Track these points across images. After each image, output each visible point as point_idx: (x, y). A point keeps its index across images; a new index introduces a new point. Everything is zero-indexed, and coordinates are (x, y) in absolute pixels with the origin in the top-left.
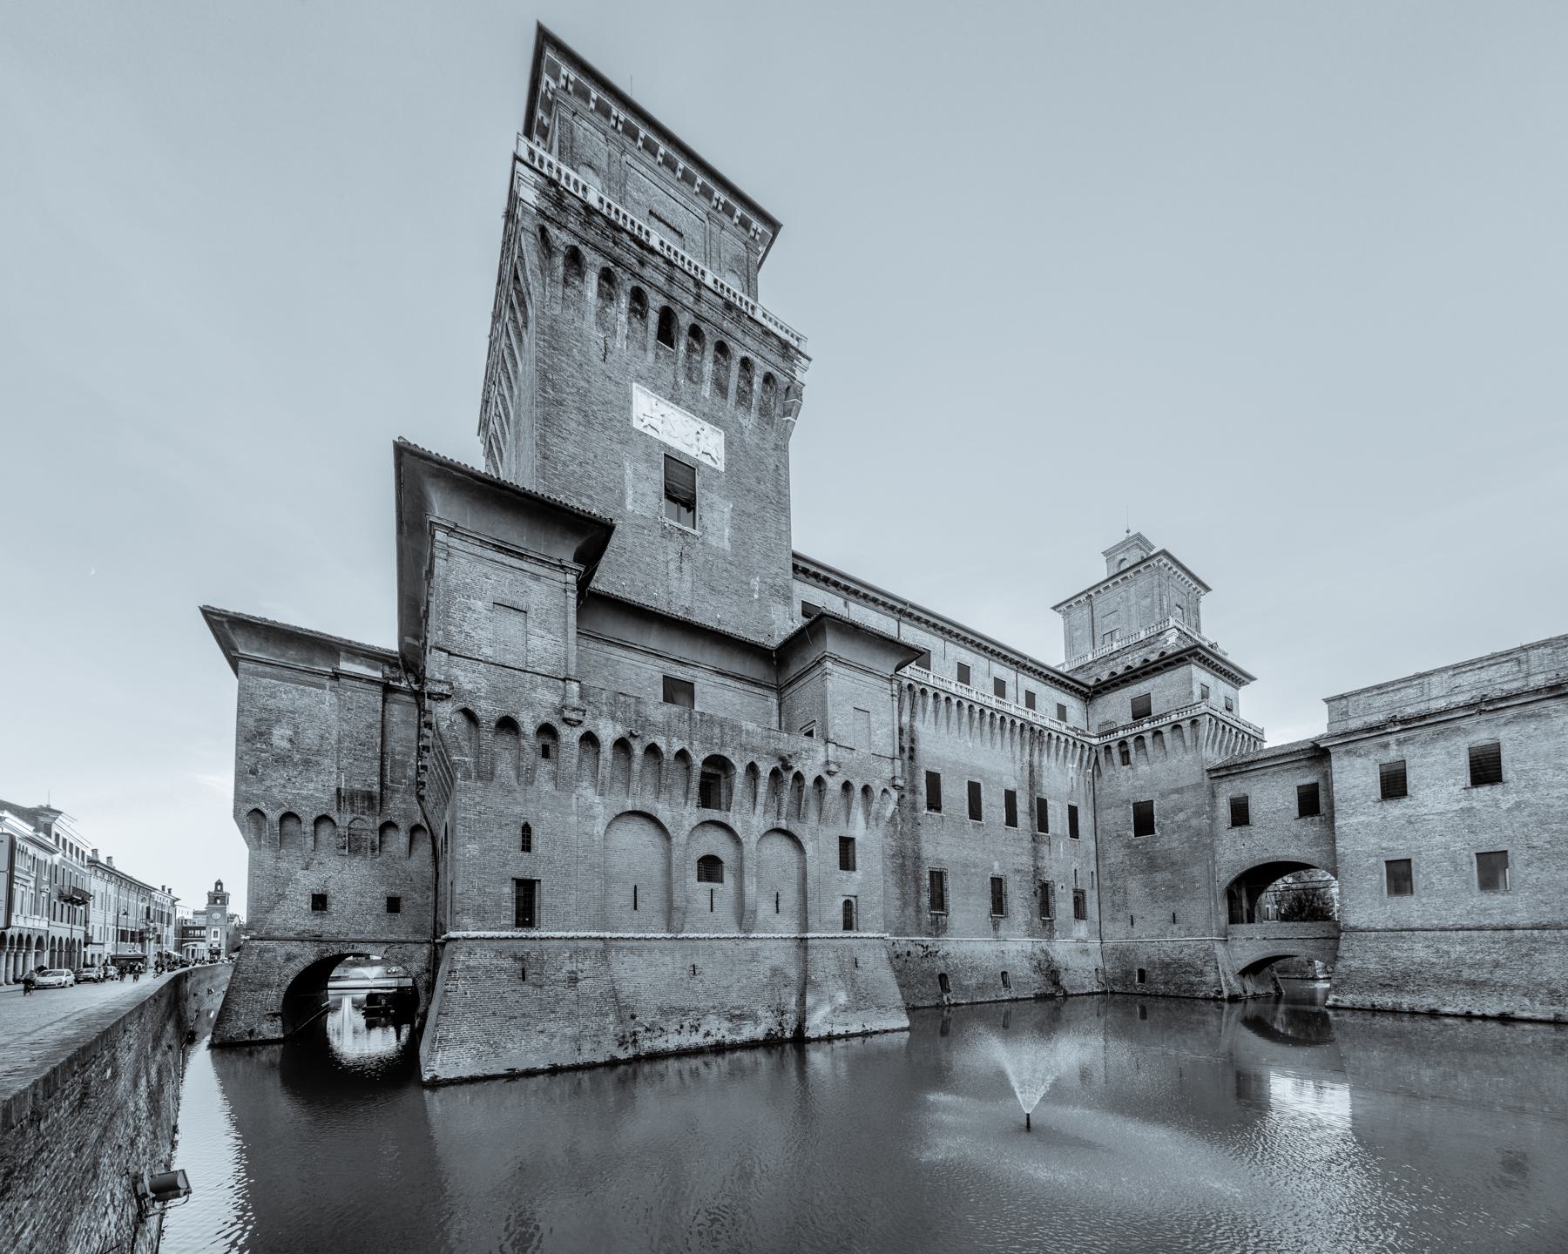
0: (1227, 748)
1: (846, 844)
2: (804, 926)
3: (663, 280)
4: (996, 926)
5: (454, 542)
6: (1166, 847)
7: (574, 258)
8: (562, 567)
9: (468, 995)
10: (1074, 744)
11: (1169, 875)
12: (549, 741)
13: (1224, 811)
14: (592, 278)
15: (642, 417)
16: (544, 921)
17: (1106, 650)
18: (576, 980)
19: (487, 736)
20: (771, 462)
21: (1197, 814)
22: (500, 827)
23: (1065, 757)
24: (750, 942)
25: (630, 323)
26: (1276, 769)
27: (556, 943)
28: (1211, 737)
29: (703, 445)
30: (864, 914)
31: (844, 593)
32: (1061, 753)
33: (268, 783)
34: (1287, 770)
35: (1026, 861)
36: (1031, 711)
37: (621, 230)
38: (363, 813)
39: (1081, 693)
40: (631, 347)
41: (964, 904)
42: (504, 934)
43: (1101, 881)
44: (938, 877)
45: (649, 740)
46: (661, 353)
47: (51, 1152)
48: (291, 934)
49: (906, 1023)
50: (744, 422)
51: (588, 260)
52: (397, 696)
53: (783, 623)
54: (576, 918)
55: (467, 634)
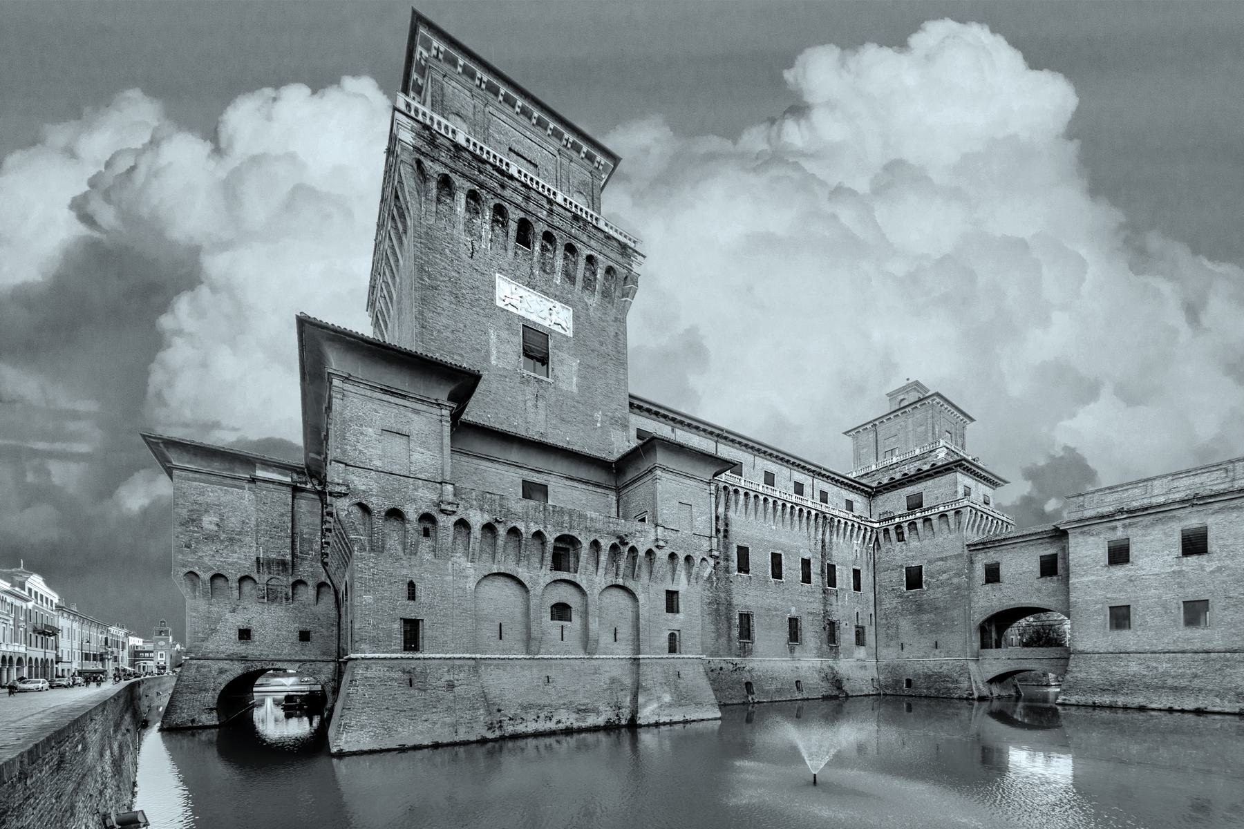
0: (984, 529)
1: (672, 596)
2: (637, 650)
3: (521, 199)
4: (792, 650)
5: (348, 387)
6: (932, 597)
7: (445, 183)
8: (439, 405)
9: (367, 696)
10: (859, 527)
11: (933, 616)
12: (429, 525)
13: (980, 572)
14: (461, 198)
15: (504, 298)
16: (426, 647)
17: (888, 463)
18: (453, 686)
19: (379, 522)
20: (612, 330)
21: (958, 575)
22: (391, 584)
23: (851, 536)
24: (593, 661)
25: (493, 230)
26: (1023, 544)
27: (436, 661)
28: (971, 522)
29: (554, 318)
30: (684, 641)
31: (672, 423)
32: (848, 533)
33: (200, 554)
34: (1032, 545)
35: (817, 607)
36: (824, 504)
37: (485, 162)
38: (278, 574)
39: (866, 492)
40: (494, 248)
41: (767, 636)
42: (394, 656)
43: (878, 619)
44: (746, 618)
45: (511, 525)
46: (519, 252)
47: (36, 799)
48: (223, 656)
49: (719, 715)
50: (589, 302)
51: (457, 184)
52: (303, 494)
53: (621, 443)
54: (453, 645)
55: (360, 451)
